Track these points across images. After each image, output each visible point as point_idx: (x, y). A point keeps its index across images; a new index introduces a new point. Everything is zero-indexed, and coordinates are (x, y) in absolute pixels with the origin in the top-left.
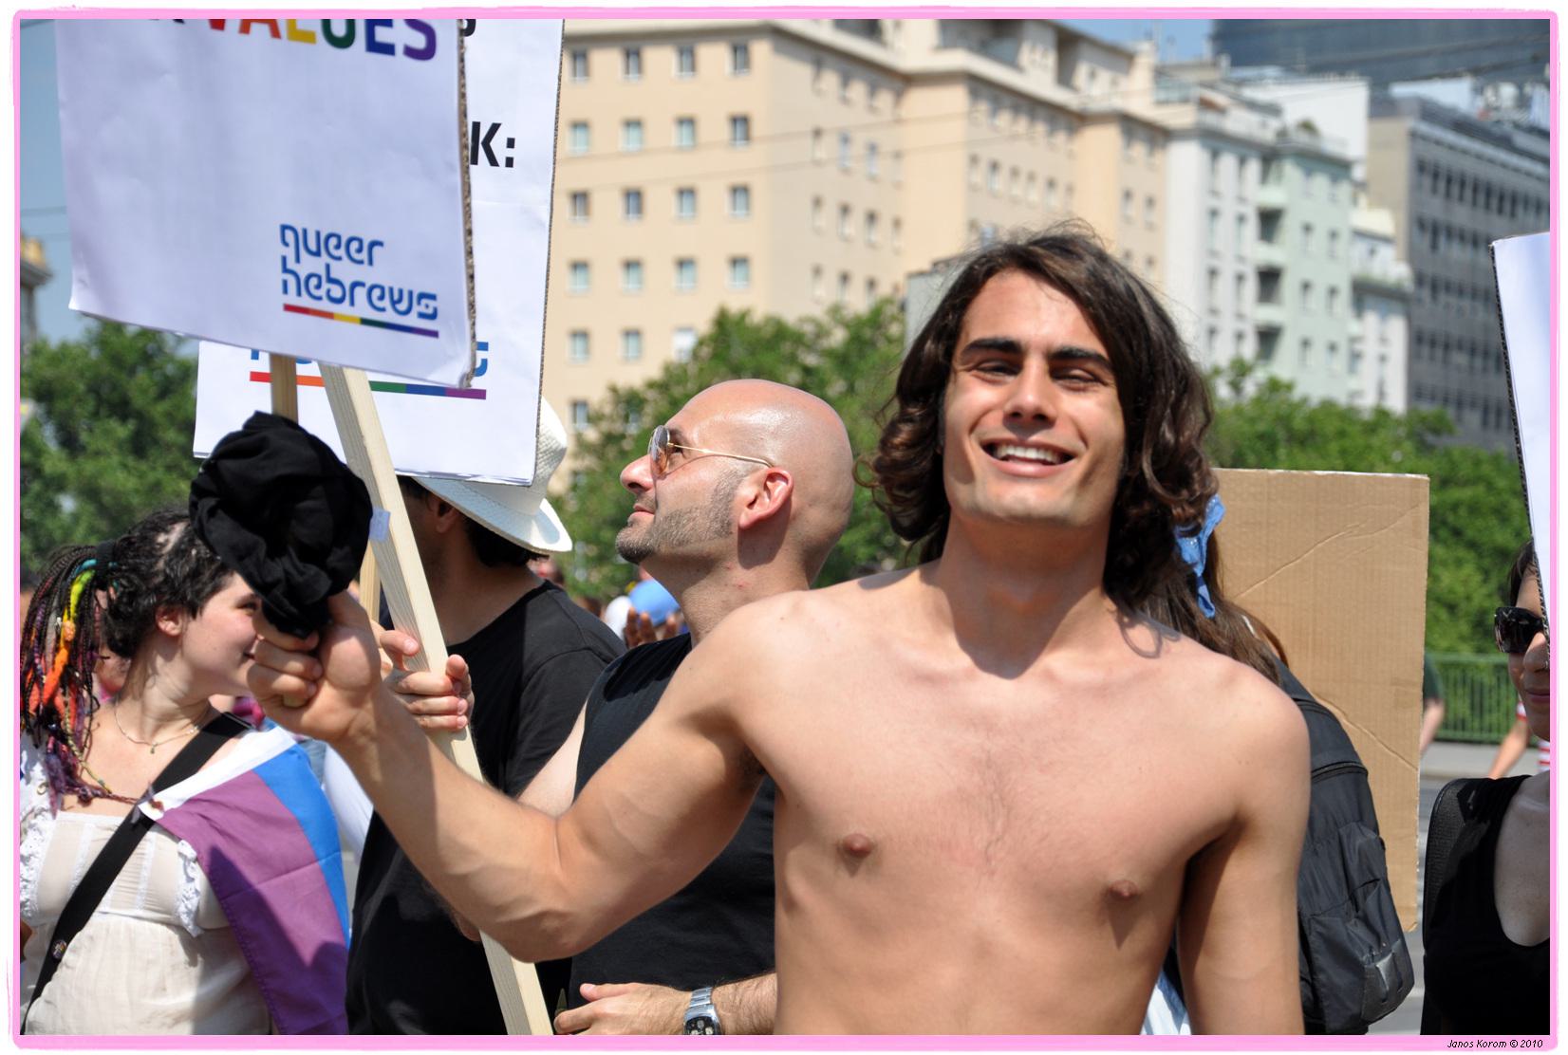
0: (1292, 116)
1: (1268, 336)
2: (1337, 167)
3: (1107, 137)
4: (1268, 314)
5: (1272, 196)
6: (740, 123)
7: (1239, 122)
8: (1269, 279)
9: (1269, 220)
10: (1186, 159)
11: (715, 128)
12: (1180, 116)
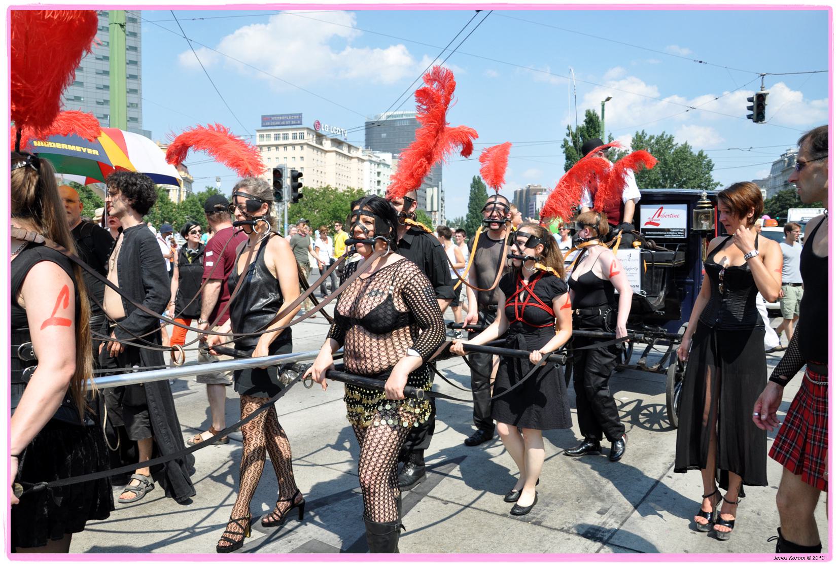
0: (381, 159)
1: (379, 191)
2: (388, 166)
3: (356, 160)
4: (379, 187)
5: (379, 170)
6: (302, 158)
7: (374, 159)
8: (379, 182)
9: (379, 173)
10: (367, 163)
11: (298, 159)
12: (366, 158)
